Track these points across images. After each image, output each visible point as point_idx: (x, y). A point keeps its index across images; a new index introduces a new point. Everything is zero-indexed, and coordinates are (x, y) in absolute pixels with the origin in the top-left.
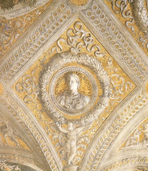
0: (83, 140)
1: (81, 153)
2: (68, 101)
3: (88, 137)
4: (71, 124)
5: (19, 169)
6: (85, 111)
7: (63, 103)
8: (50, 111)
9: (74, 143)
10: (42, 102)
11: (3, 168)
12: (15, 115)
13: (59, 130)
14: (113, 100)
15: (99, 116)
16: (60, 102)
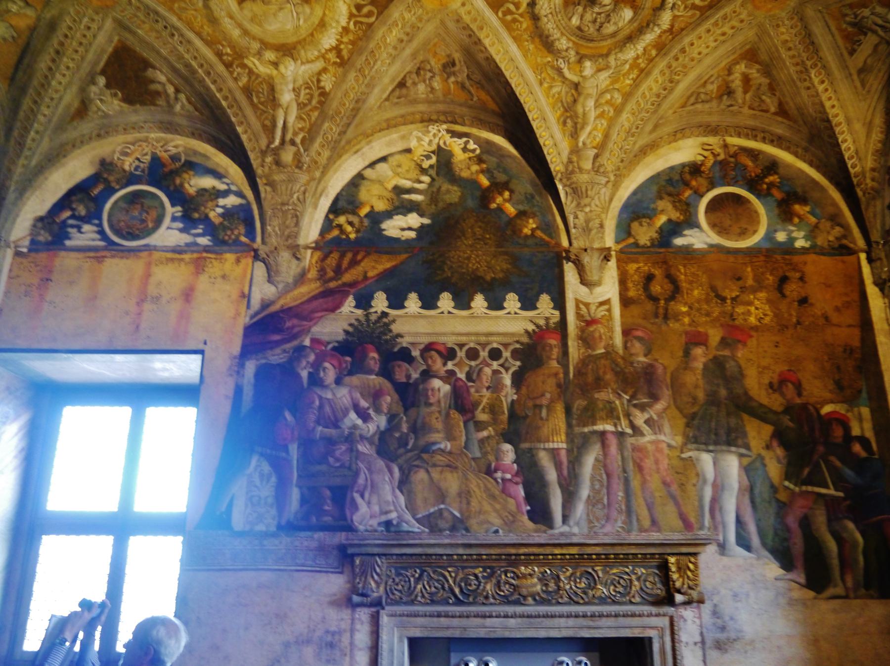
0: (608, 96)
1: (602, 124)
2: (588, 17)
3: (618, 90)
4: (588, 64)
5: (476, 146)
6: (621, 36)
7: (575, 21)
8: (548, 37)
9: (591, 103)
10: (535, 18)
11: (445, 143)
12: (476, 43)
13: (564, 77)
14: (678, 16)
15: (645, 49)
16: (570, 19)
